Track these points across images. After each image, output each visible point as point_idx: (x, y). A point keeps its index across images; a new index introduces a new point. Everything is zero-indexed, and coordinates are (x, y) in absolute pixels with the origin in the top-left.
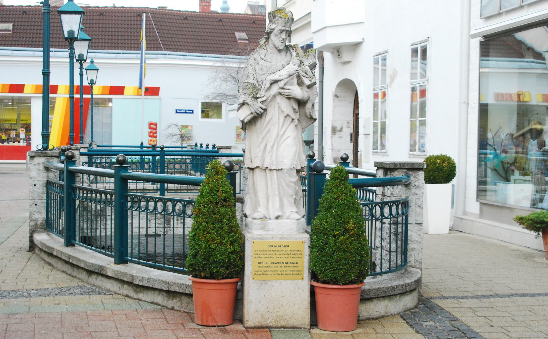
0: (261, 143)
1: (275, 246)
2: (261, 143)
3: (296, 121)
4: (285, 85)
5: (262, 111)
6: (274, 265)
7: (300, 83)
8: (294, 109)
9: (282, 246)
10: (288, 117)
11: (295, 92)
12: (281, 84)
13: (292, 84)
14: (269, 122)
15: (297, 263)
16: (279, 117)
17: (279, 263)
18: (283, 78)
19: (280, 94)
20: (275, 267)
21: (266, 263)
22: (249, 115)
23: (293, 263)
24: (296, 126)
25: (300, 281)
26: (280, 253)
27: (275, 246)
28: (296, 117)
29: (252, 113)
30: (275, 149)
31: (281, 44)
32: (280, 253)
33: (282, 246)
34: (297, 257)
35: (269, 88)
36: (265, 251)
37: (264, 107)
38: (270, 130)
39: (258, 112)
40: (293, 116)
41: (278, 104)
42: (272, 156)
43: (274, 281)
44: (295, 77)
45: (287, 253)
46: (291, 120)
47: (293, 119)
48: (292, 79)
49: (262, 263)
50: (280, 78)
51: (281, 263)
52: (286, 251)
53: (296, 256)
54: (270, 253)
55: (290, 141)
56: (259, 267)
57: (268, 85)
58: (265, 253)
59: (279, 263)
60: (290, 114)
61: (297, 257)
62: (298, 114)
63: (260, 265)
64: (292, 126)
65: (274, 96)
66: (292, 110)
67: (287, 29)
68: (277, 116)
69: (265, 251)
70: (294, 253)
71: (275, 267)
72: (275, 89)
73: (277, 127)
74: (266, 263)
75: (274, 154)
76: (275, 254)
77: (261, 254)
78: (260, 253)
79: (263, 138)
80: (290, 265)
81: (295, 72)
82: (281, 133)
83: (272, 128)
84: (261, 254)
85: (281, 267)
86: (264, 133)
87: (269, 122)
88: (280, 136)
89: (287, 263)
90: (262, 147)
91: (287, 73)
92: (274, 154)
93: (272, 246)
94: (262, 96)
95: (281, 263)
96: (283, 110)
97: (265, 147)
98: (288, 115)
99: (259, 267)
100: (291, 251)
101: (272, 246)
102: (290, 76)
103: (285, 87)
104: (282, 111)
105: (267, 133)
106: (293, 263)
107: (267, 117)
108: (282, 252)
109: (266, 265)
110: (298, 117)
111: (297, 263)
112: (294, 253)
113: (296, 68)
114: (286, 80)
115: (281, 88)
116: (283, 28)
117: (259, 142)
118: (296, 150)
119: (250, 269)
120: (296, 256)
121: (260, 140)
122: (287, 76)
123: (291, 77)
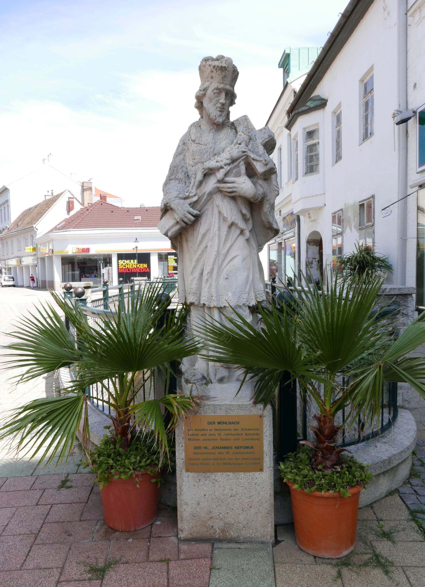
0: (194, 268)
1: (219, 423)
2: (194, 268)
3: (247, 233)
4: (226, 175)
5: (192, 218)
6: (217, 451)
7: (251, 173)
8: (244, 216)
9: (230, 423)
10: (233, 228)
11: (243, 186)
12: (220, 175)
13: (238, 175)
14: (204, 235)
15: (252, 447)
16: (219, 227)
17: (224, 448)
18: (222, 164)
19: (219, 191)
20: (219, 453)
21: (206, 448)
22: (172, 227)
23: (246, 448)
24: (248, 240)
25: (257, 474)
26: (226, 432)
27: (219, 423)
28: (247, 227)
29: (177, 223)
30: (214, 277)
31: (219, 113)
32: (226, 432)
33: (230, 423)
34: (253, 439)
35: (201, 183)
36: (203, 430)
37: (195, 212)
38: (207, 247)
39: (186, 220)
40: (241, 224)
41: (218, 206)
42: (211, 285)
43: (219, 474)
44: (242, 163)
45: (236, 432)
46: (238, 232)
47: (242, 232)
48: (238, 166)
49: (200, 448)
50: (219, 164)
51: (228, 448)
52: (235, 430)
53: (251, 437)
54: (212, 432)
55: (237, 262)
56: (195, 453)
57: (199, 177)
58: (203, 432)
59: (224, 448)
60: (236, 222)
61: (253, 439)
62: (250, 221)
63: (196, 451)
64: (241, 241)
65: (211, 194)
66: (240, 217)
67: (228, 87)
68: (217, 225)
69: (203, 430)
70: (248, 432)
71: (219, 453)
72: (211, 184)
73: (216, 241)
74: (206, 448)
75: (214, 284)
76: (219, 435)
77: (198, 435)
78: (196, 432)
79: (198, 261)
80: (242, 450)
81: (241, 154)
82: (224, 251)
83: (210, 244)
84: (198, 435)
85: (228, 453)
86: (199, 252)
87: (204, 235)
88: (222, 257)
89: (237, 448)
90: (197, 274)
91: (228, 156)
92: (214, 284)
93: (214, 423)
94: (191, 195)
95: (228, 448)
96: (225, 215)
97: (202, 274)
98: (233, 224)
99: (195, 453)
100: (242, 429)
101: (214, 423)
102: (233, 161)
103: (227, 179)
104: (225, 219)
105: (203, 251)
106: (246, 448)
107: (202, 227)
108: (229, 432)
109: (206, 451)
110: (250, 226)
111: (252, 447)
112: (248, 432)
113: (243, 147)
114: (228, 168)
115: (219, 181)
116: (221, 86)
117: (192, 265)
118: (248, 277)
119: (183, 456)
120: (251, 437)
121: (193, 264)
122: (228, 162)
123: (235, 164)
